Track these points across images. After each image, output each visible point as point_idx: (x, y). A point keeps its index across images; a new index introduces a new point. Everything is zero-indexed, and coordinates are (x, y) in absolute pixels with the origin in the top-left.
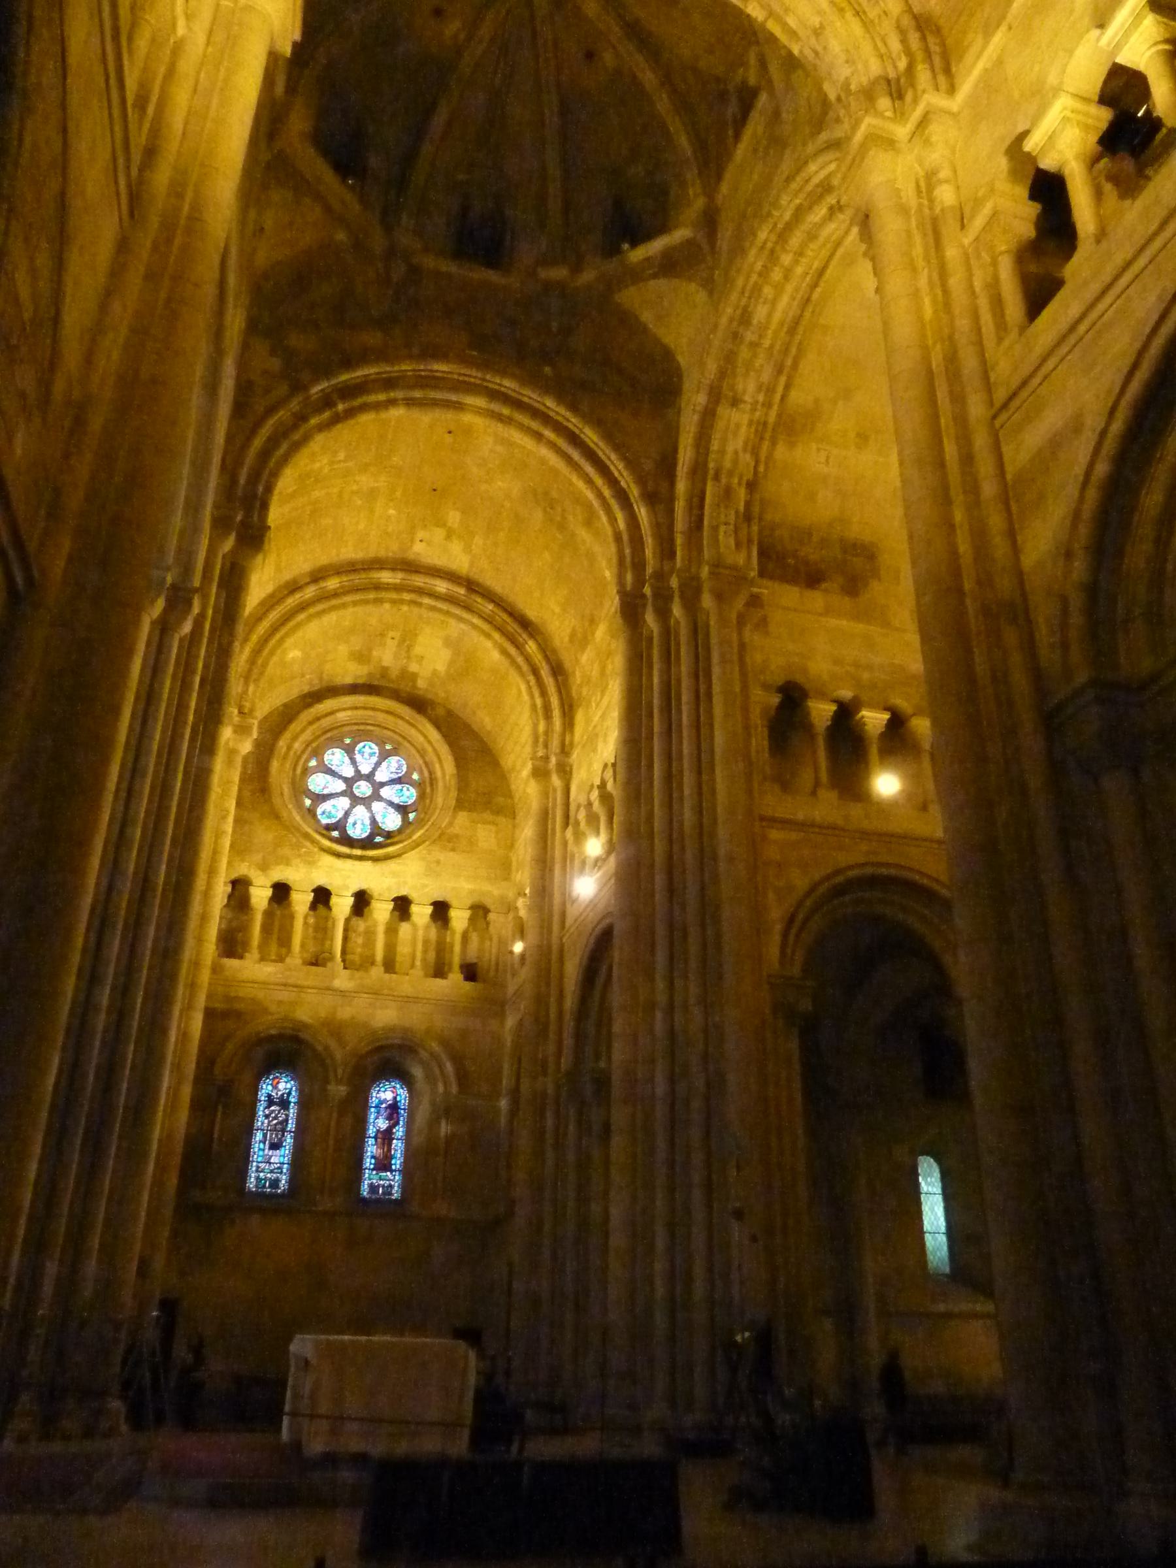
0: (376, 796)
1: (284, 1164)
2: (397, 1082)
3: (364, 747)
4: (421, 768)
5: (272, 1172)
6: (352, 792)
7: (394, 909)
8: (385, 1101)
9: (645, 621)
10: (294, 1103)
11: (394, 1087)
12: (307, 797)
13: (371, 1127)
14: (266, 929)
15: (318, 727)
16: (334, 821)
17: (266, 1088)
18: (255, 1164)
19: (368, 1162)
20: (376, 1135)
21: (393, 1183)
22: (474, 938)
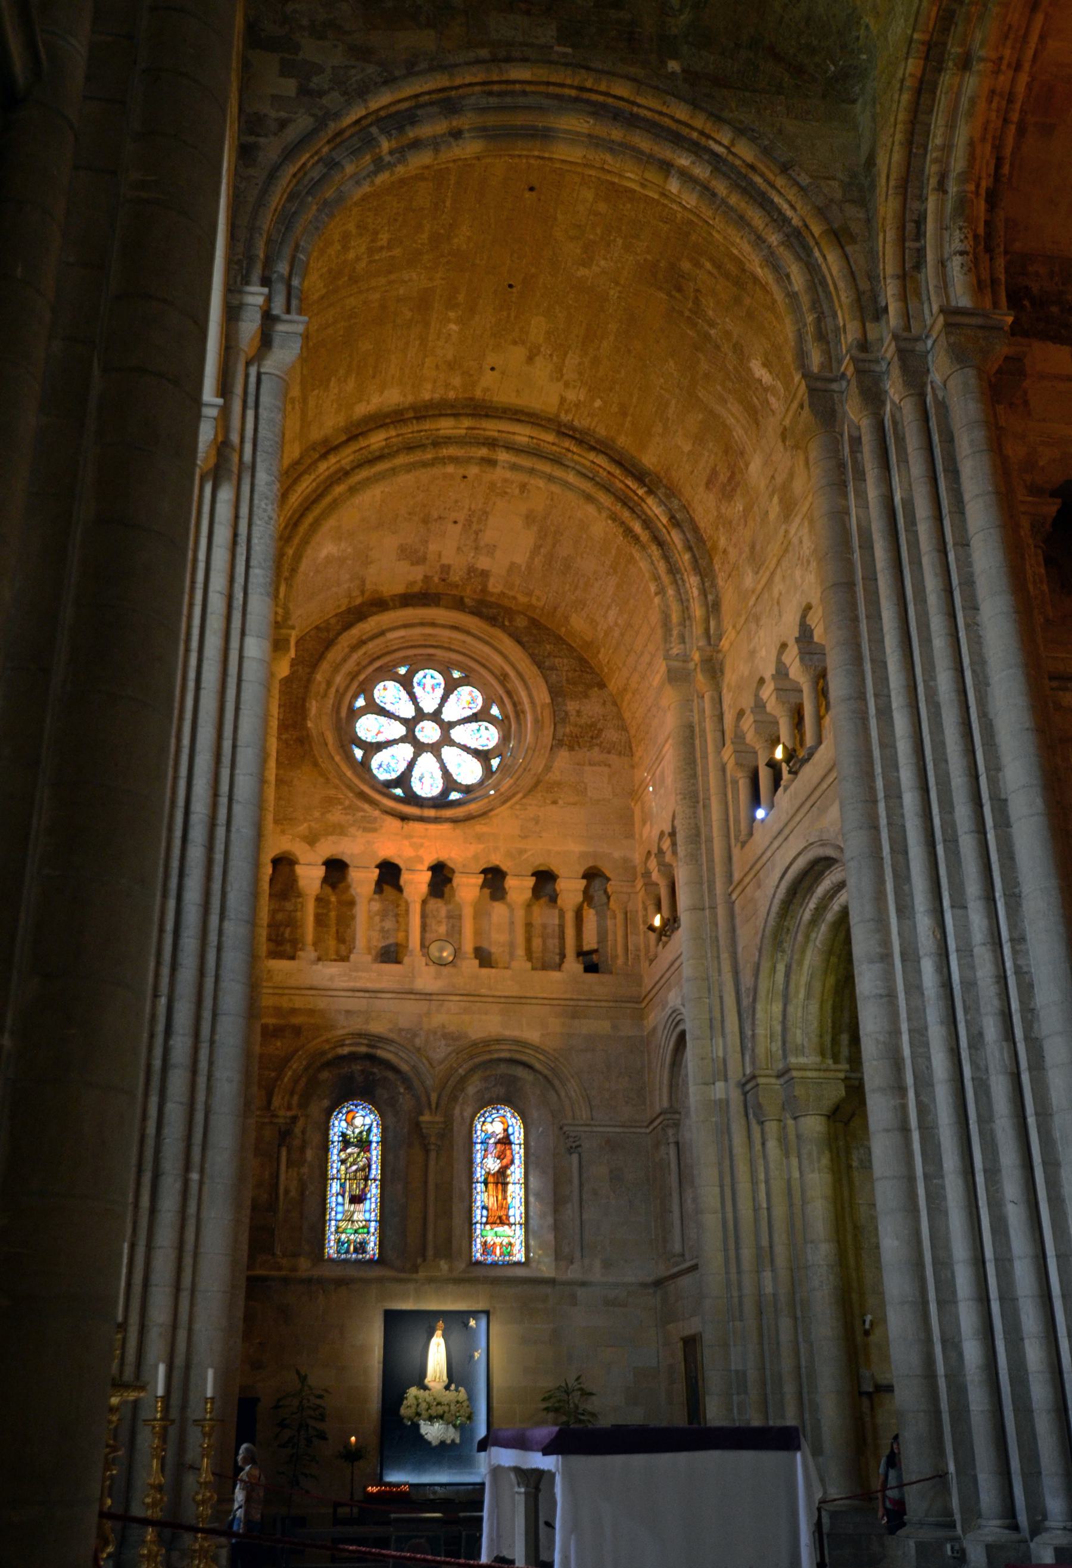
0: (446, 740)
1: (369, 1221)
2: (507, 1109)
3: (425, 677)
4: (501, 698)
5: (356, 1232)
6: (415, 737)
7: (484, 885)
8: (493, 1134)
9: (845, 413)
10: (377, 1142)
11: (504, 1116)
12: (357, 746)
13: (479, 1169)
14: (320, 921)
15: (365, 654)
16: (394, 776)
17: (338, 1126)
18: (333, 1223)
19: (478, 1215)
20: (486, 1179)
21: (513, 1241)
22: (590, 917)
